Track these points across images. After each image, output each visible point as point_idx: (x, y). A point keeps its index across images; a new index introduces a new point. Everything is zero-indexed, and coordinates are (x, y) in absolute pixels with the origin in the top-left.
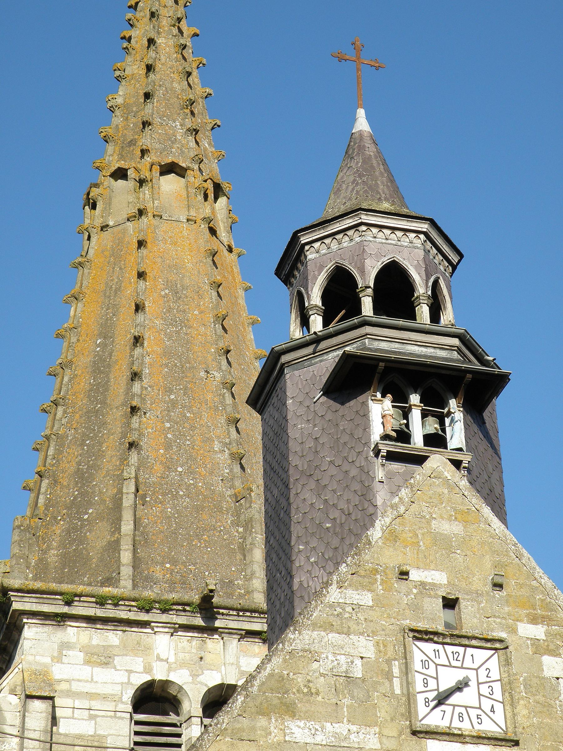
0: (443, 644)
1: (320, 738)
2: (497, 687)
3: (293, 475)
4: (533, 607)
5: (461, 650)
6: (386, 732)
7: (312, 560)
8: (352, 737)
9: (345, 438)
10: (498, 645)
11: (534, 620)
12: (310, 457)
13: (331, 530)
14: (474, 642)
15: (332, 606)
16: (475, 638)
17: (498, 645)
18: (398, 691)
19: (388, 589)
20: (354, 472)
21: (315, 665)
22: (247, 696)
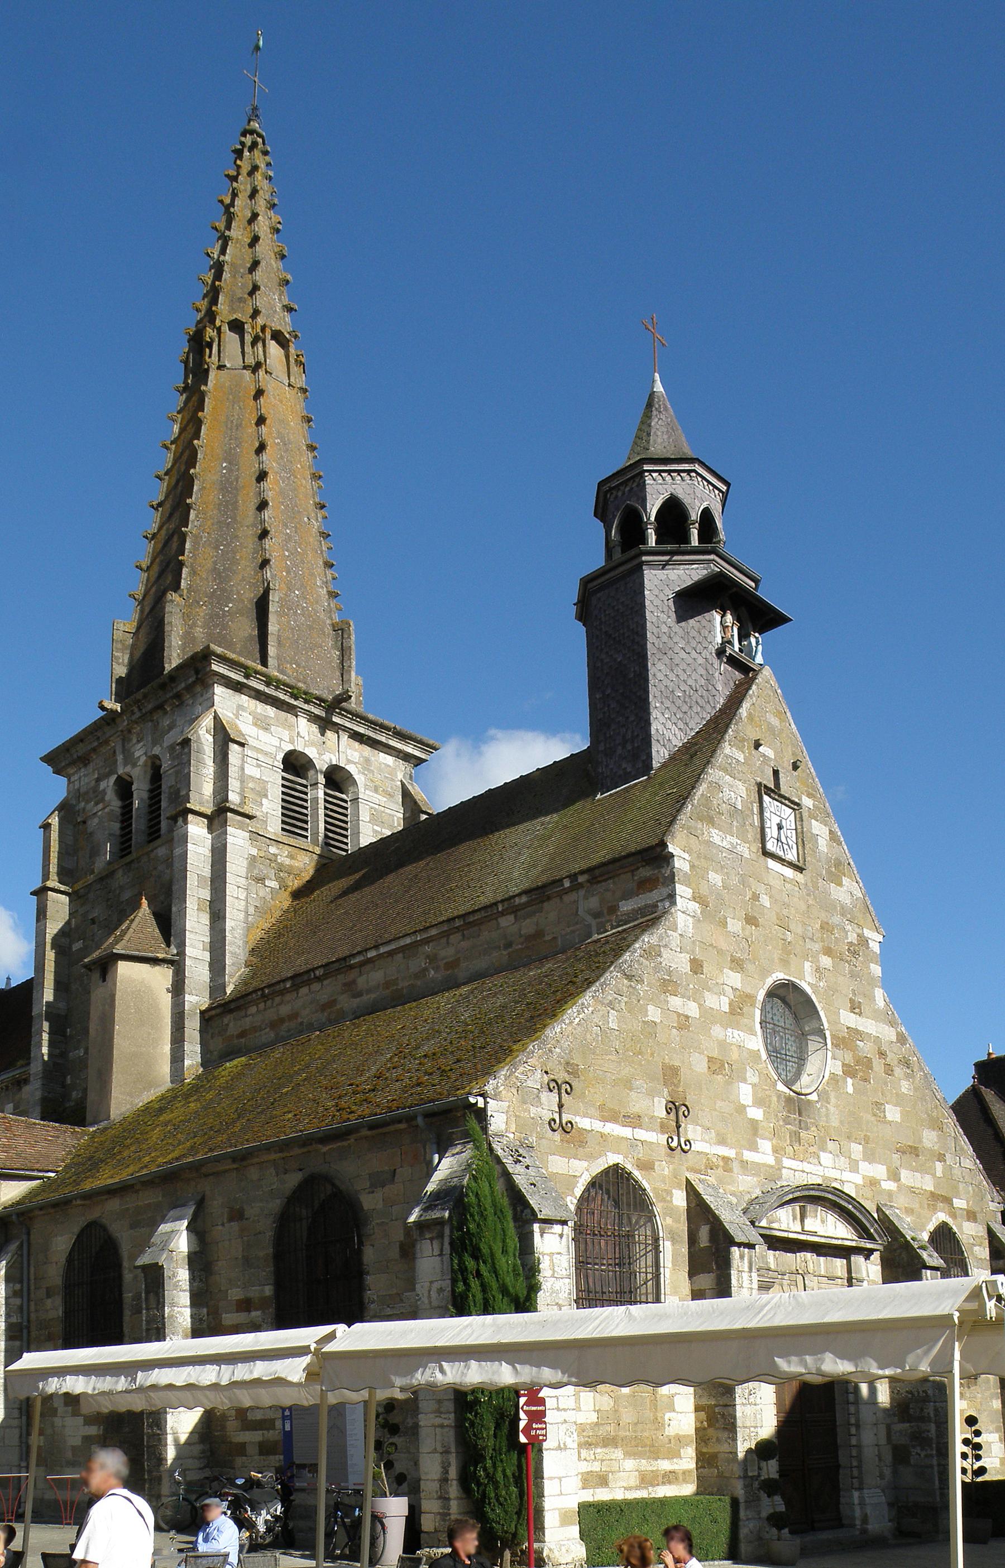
0: (774, 799)
1: (725, 844)
2: (794, 832)
3: (650, 649)
4: (808, 786)
5: (779, 804)
6: (752, 848)
7: (666, 716)
8: (738, 847)
9: (693, 633)
10: (796, 807)
11: (809, 796)
12: (665, 639)
13: (682, 699)
14: (787, 802)
15: (727, 756)
16: (789, 800)
17: (796, 807)
18: (756, 824)
19: (750, 754)
20: (701, 661)
21: (721, 795)
22: (692, 805)
